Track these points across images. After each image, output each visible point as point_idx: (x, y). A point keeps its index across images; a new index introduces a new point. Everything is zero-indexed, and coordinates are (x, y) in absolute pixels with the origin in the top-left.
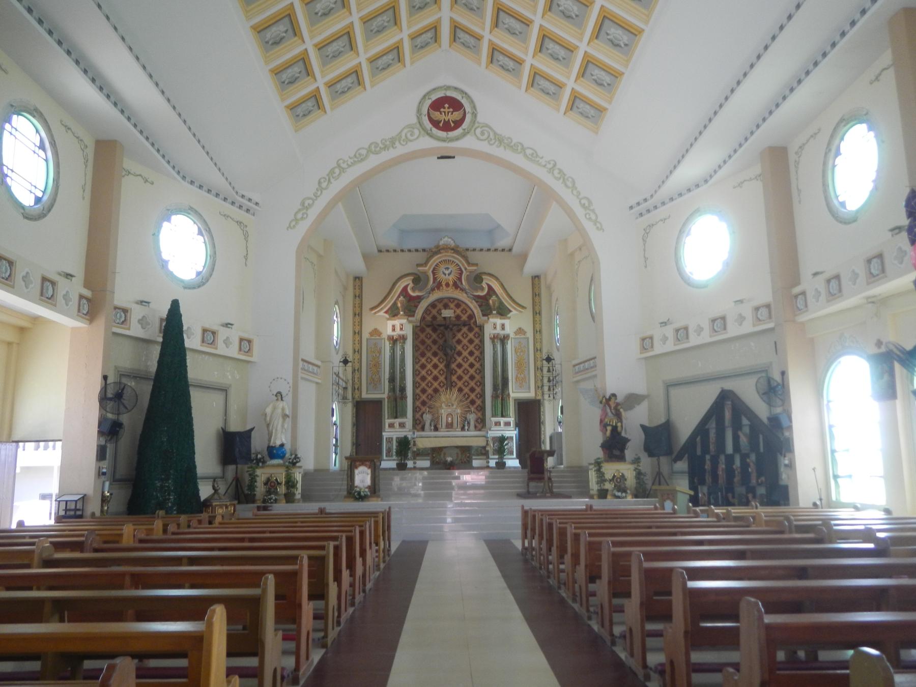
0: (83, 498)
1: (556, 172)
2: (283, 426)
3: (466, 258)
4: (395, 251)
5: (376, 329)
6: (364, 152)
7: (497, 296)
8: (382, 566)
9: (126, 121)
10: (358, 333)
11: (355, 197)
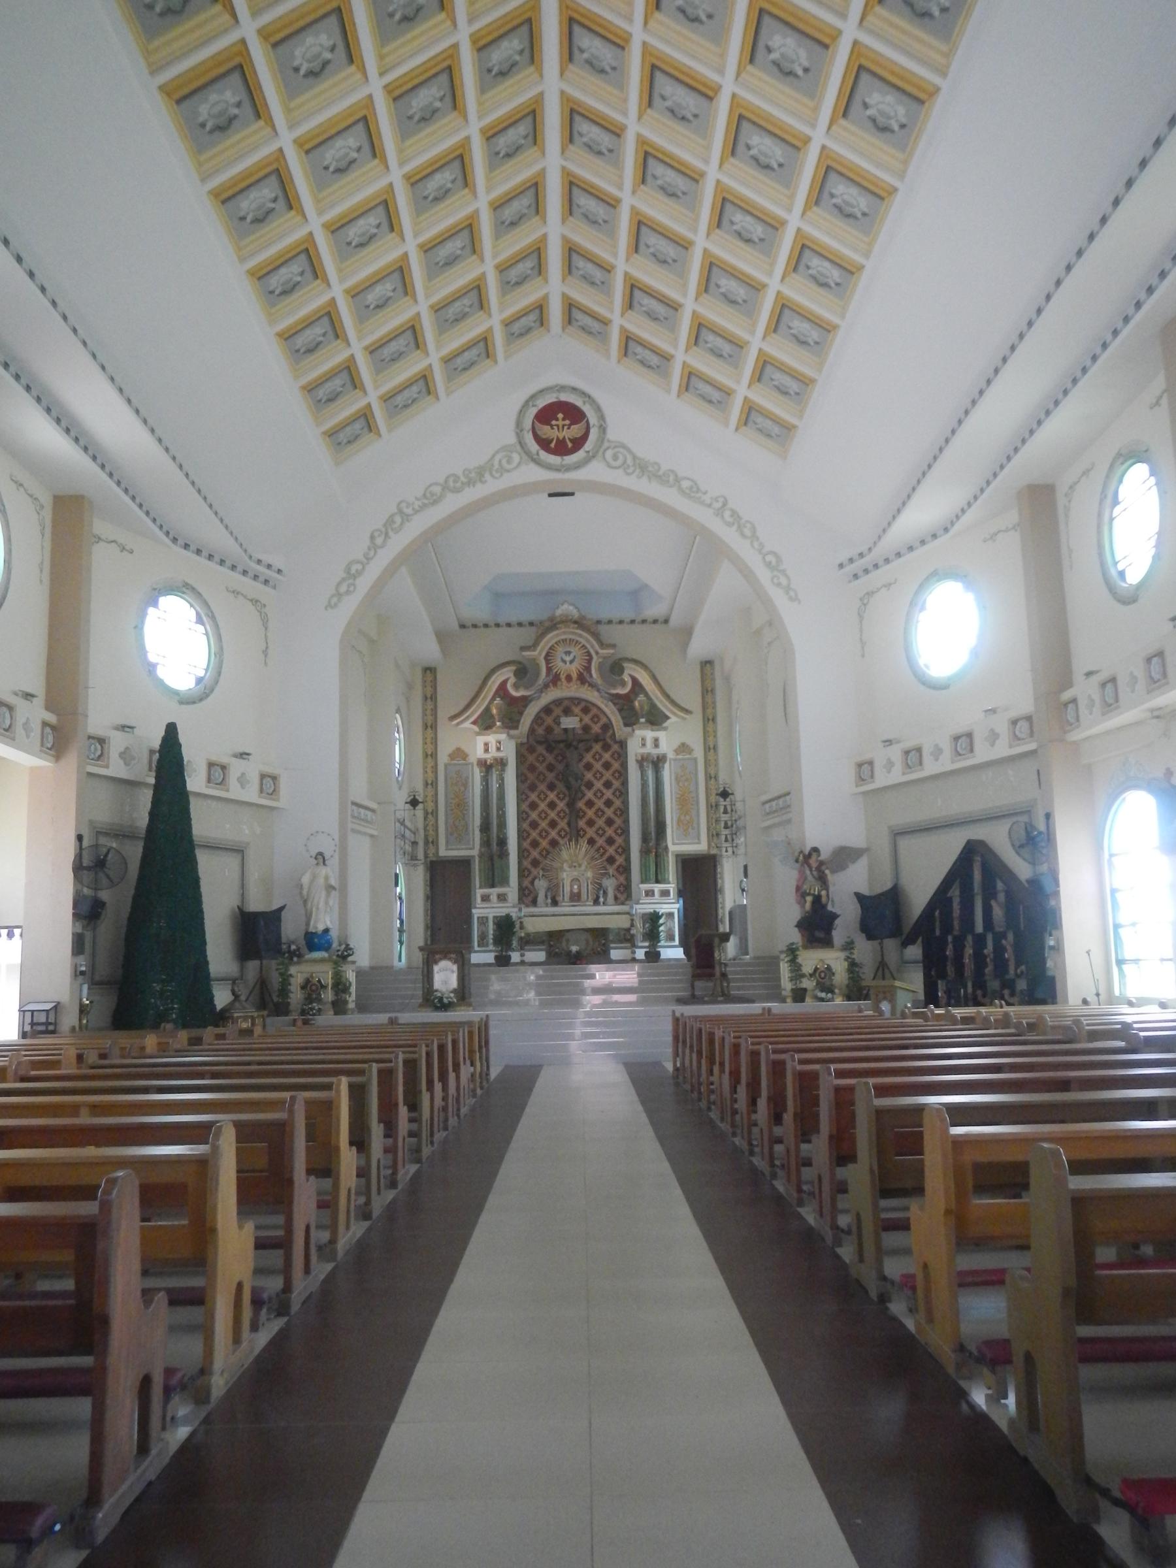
0: (55, 1007)
1: (727, 514)
2: (327, 903)
3: (596, 636)
4: (486, 626)
5: (458, 749)
6: (437, 489)
7: (646, 695)
8: (479, 1092)
9: (98, 470)
10: (431, 755)
11: (426, 557)
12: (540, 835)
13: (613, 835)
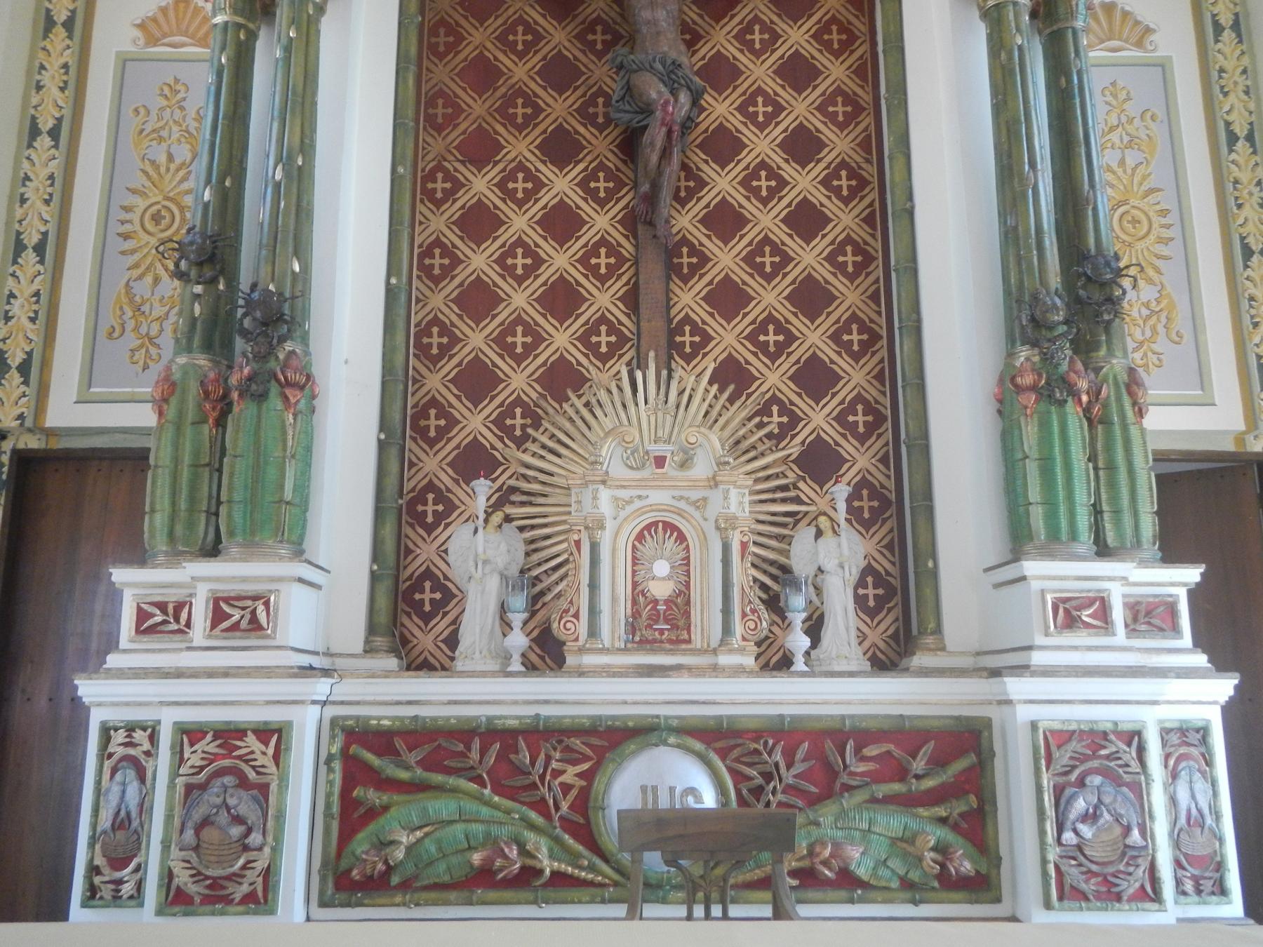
12: (501, 341)
13: (828, 352)
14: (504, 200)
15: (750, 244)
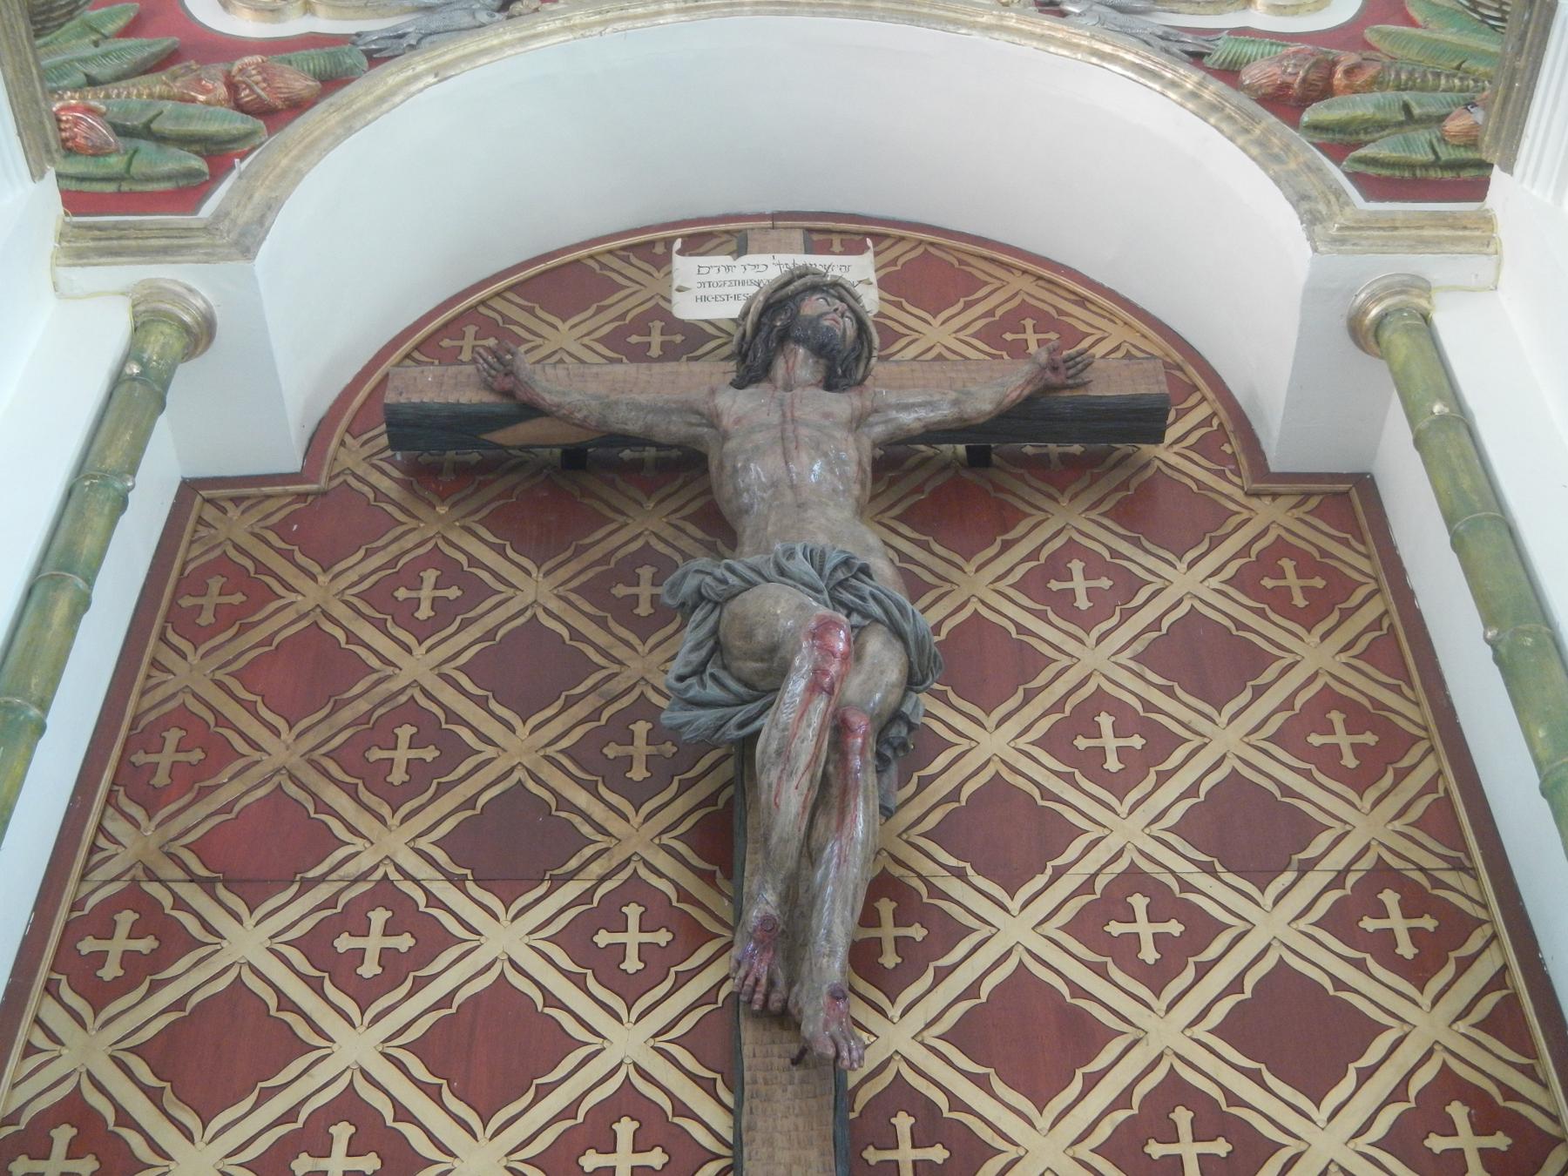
14: (316, 987)
15: (1123, 1100)
